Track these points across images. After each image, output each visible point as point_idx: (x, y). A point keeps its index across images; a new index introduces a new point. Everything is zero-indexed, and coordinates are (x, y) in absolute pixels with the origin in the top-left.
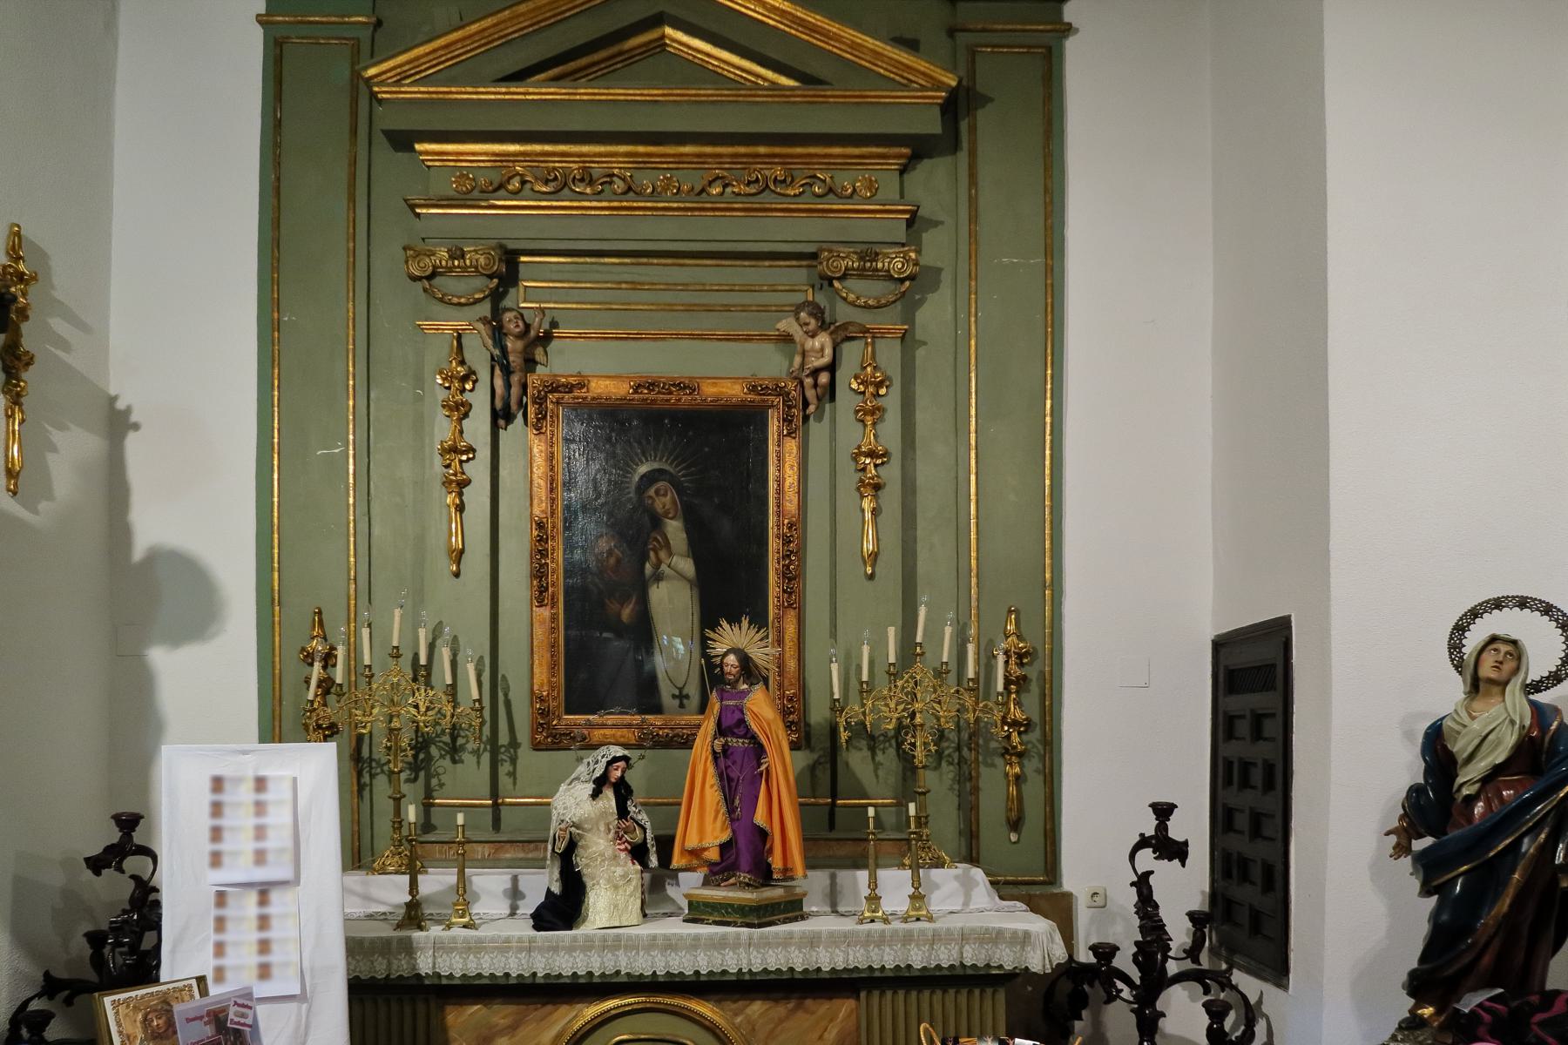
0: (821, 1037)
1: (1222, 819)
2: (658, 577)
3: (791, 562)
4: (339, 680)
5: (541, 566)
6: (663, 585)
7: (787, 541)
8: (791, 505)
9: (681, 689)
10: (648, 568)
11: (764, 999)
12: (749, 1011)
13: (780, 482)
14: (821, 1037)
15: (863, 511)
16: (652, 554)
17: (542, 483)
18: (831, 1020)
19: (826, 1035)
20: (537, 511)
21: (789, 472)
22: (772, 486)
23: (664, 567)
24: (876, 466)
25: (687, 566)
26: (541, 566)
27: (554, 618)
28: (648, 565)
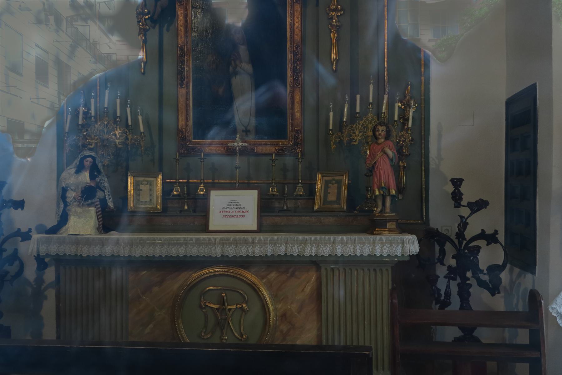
0: (303, 290)
1: (509, 196)
2: (236, 73)
3: (298, 65)
4: (93, 114)
5: (182, 68)
6: (238, 77)
7: (295, 54)
8: (297, 38)
9: (246, 127)
10: (231, 68)
11: (293, 346)
12: (269, 277)
13: (292, 25)
14: (303, 290)
15: (331, 39)
16: (233, 62)
17: (182, 28)
18: (308, 282)
19: (305, 290)
20: (180, 42)
21: (296, 20)
22: (288, 27)
23: (238, 69)
24: (337, 16)
25: (248, 67)
26: (182, 68)
27: (188, 93)
28: (231, 68)
